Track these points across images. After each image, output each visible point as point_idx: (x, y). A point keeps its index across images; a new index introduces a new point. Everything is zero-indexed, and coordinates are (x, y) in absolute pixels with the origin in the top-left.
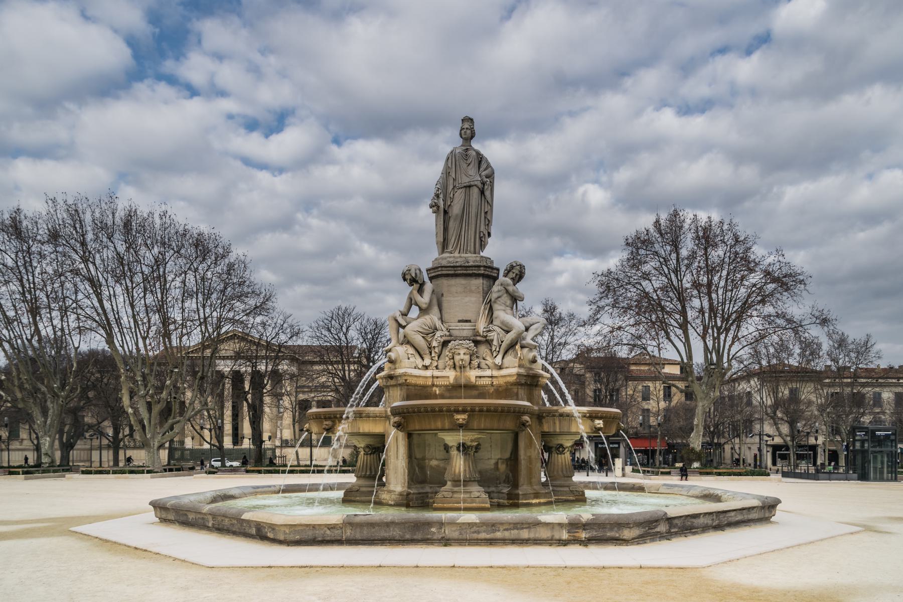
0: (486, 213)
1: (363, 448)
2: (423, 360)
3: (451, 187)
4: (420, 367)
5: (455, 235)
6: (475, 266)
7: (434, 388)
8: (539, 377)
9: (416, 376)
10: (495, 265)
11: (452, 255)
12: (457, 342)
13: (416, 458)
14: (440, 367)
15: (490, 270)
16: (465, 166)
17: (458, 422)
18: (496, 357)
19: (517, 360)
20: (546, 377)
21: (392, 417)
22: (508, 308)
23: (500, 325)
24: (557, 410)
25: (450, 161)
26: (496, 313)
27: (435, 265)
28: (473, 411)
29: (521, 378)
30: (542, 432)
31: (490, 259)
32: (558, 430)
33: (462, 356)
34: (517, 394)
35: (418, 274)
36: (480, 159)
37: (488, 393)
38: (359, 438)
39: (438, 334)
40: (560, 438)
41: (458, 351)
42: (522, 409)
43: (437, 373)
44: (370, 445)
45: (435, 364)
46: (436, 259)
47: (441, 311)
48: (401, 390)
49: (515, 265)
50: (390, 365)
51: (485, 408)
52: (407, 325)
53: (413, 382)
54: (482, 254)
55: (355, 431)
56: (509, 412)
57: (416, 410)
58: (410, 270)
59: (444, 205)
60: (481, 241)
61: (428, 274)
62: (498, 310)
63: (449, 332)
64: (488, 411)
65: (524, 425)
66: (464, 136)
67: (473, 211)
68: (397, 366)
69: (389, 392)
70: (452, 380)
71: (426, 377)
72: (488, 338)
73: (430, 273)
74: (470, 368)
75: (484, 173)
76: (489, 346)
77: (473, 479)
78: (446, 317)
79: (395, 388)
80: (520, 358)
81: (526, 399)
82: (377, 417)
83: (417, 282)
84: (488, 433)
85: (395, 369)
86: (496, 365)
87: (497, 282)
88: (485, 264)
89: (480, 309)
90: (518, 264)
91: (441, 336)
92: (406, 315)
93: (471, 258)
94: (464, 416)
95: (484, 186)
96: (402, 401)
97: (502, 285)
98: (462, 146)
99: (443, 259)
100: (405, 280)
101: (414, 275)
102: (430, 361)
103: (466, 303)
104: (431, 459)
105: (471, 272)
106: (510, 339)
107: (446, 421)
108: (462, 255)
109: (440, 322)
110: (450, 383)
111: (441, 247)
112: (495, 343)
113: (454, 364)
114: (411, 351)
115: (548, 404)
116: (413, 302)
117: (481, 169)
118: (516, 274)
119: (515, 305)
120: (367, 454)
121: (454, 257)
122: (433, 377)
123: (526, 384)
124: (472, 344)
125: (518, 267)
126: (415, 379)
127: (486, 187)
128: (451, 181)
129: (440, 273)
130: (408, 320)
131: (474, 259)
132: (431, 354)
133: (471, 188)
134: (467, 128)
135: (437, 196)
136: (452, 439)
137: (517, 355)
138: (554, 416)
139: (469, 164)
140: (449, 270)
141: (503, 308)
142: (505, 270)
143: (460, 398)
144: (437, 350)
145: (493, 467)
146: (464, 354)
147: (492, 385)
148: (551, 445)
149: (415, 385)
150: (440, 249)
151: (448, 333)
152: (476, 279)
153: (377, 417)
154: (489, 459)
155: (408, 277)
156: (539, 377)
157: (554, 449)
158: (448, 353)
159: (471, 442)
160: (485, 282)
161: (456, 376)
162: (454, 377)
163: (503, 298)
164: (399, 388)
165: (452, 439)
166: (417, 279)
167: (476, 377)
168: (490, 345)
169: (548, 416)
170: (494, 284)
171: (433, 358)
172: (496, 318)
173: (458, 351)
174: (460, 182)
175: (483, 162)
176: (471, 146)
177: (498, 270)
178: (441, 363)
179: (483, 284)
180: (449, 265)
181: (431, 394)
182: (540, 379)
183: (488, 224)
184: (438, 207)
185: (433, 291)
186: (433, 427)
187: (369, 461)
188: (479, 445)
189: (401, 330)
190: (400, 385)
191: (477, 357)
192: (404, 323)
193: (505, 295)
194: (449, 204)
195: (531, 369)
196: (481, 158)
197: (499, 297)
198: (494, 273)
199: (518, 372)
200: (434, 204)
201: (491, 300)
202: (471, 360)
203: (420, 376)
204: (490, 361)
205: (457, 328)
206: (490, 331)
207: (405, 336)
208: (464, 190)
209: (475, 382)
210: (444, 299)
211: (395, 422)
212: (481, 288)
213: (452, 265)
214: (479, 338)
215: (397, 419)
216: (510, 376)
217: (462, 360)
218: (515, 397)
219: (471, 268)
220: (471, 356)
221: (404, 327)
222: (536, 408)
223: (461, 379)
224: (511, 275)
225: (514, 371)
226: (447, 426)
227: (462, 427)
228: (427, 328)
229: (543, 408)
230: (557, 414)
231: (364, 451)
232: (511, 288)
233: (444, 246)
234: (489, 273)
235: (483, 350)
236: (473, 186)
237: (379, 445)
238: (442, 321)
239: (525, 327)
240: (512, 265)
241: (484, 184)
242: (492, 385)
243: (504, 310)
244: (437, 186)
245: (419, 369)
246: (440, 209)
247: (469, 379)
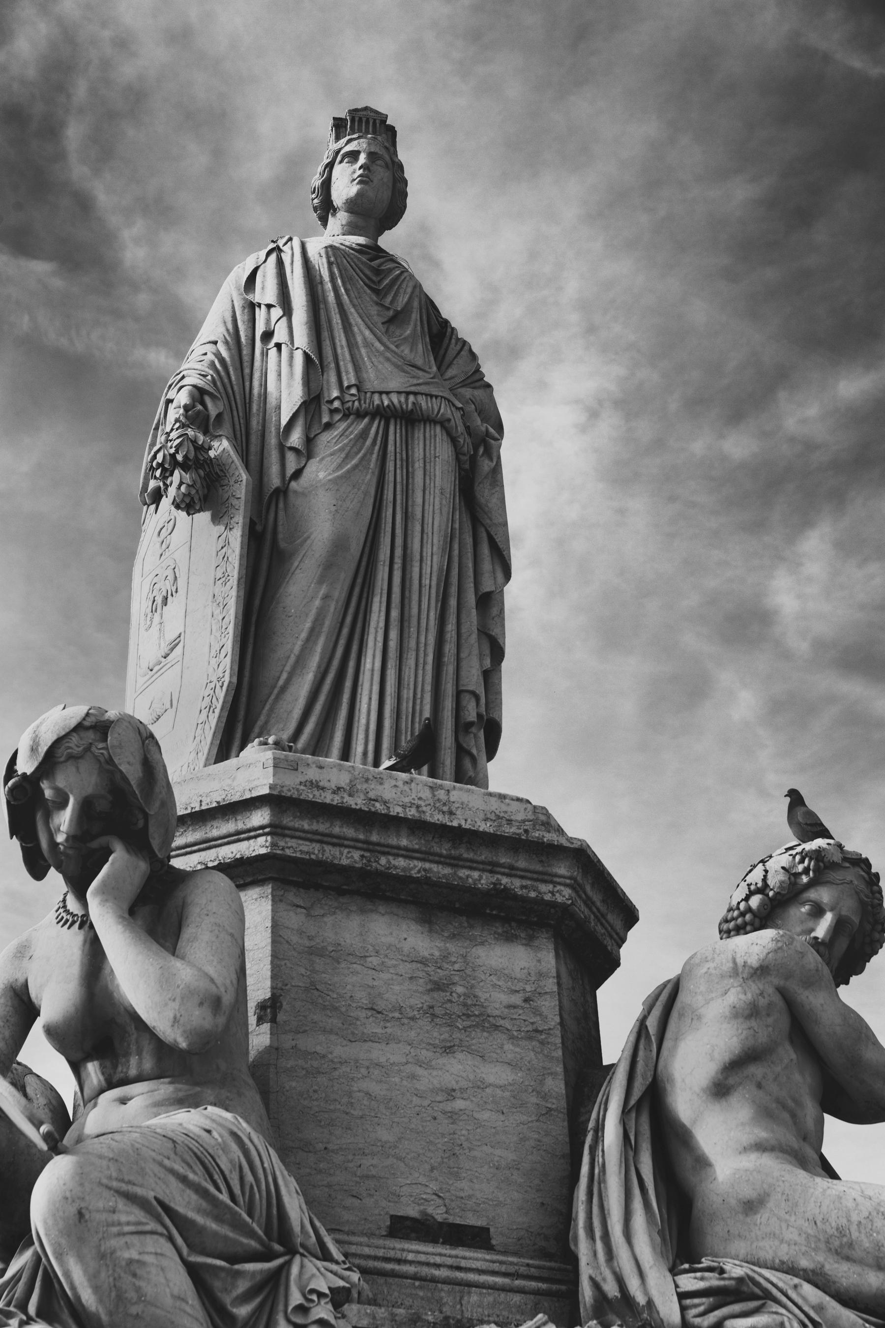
23: (804, 1263)
103: (451, 1094)
140: (323, 839)
193: (788, 1054)
219: (484, 855)
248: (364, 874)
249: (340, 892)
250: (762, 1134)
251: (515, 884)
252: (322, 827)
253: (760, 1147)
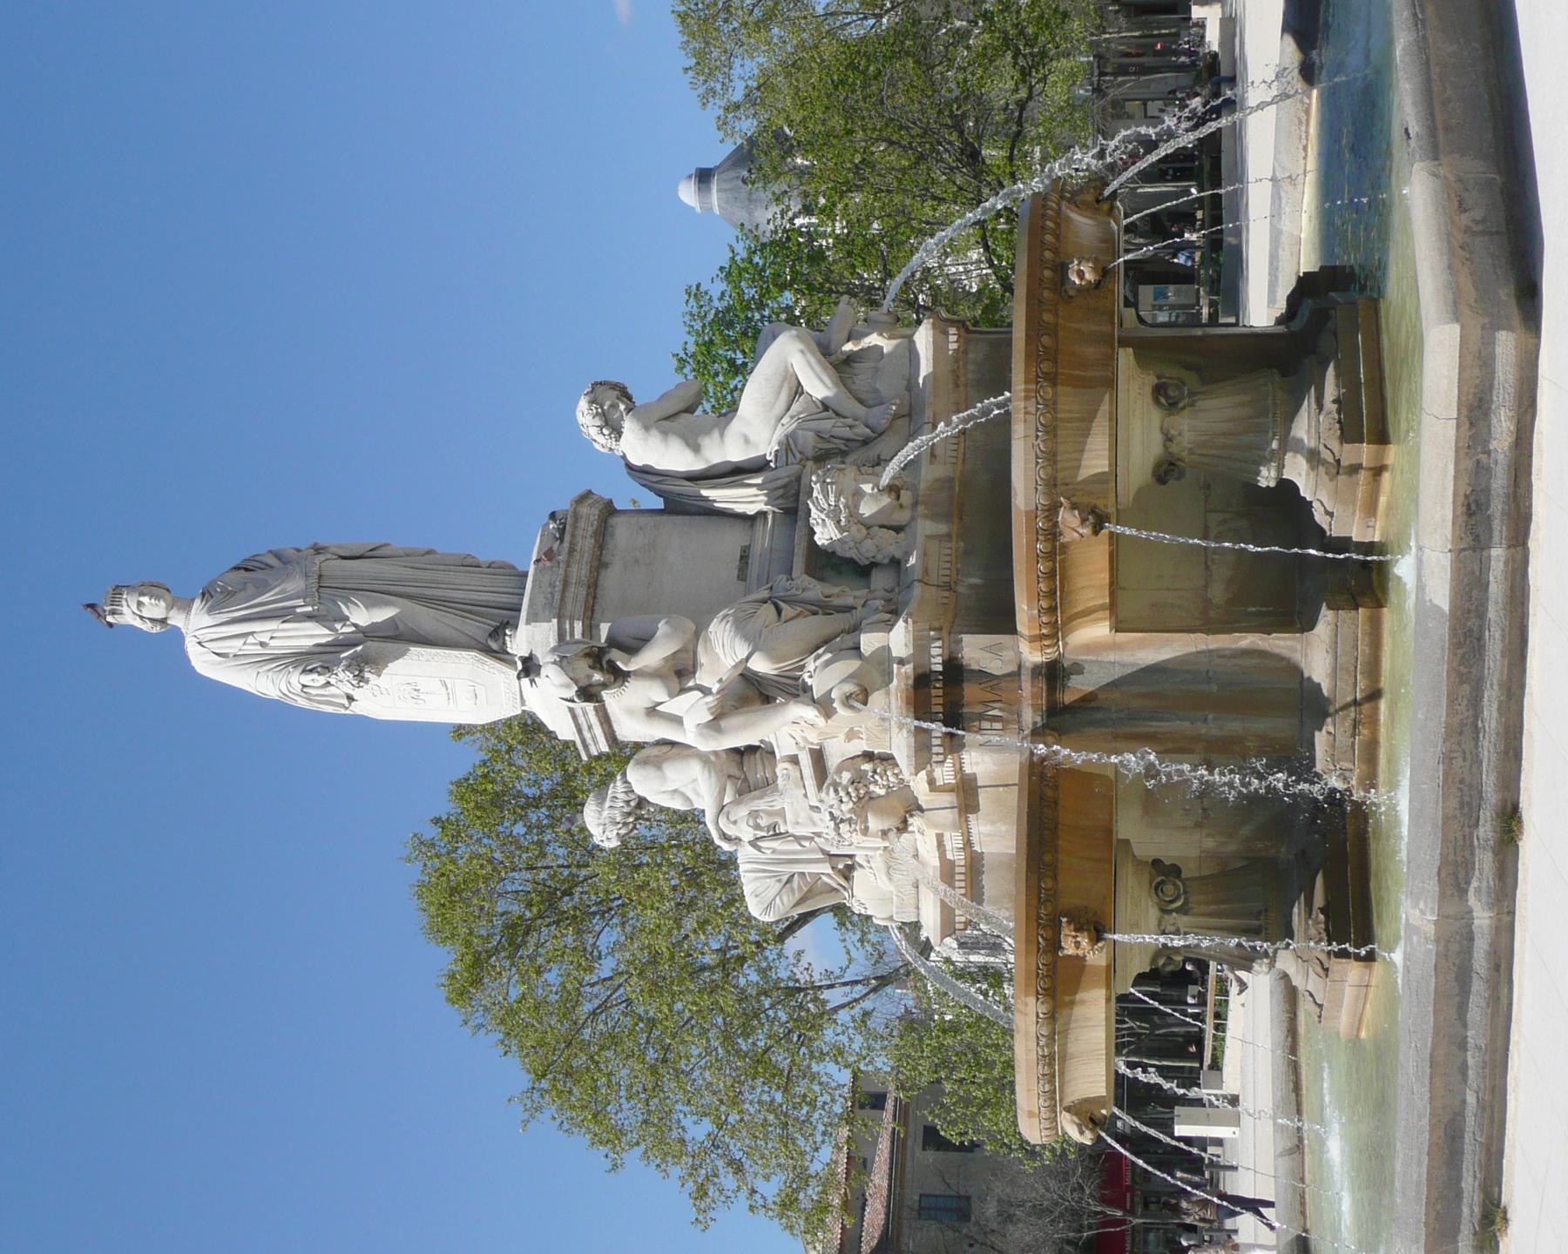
7: (961, 589)
104: (1207, 601)
161: (926, 517)
250: (716, 434)
253: (722, 435)
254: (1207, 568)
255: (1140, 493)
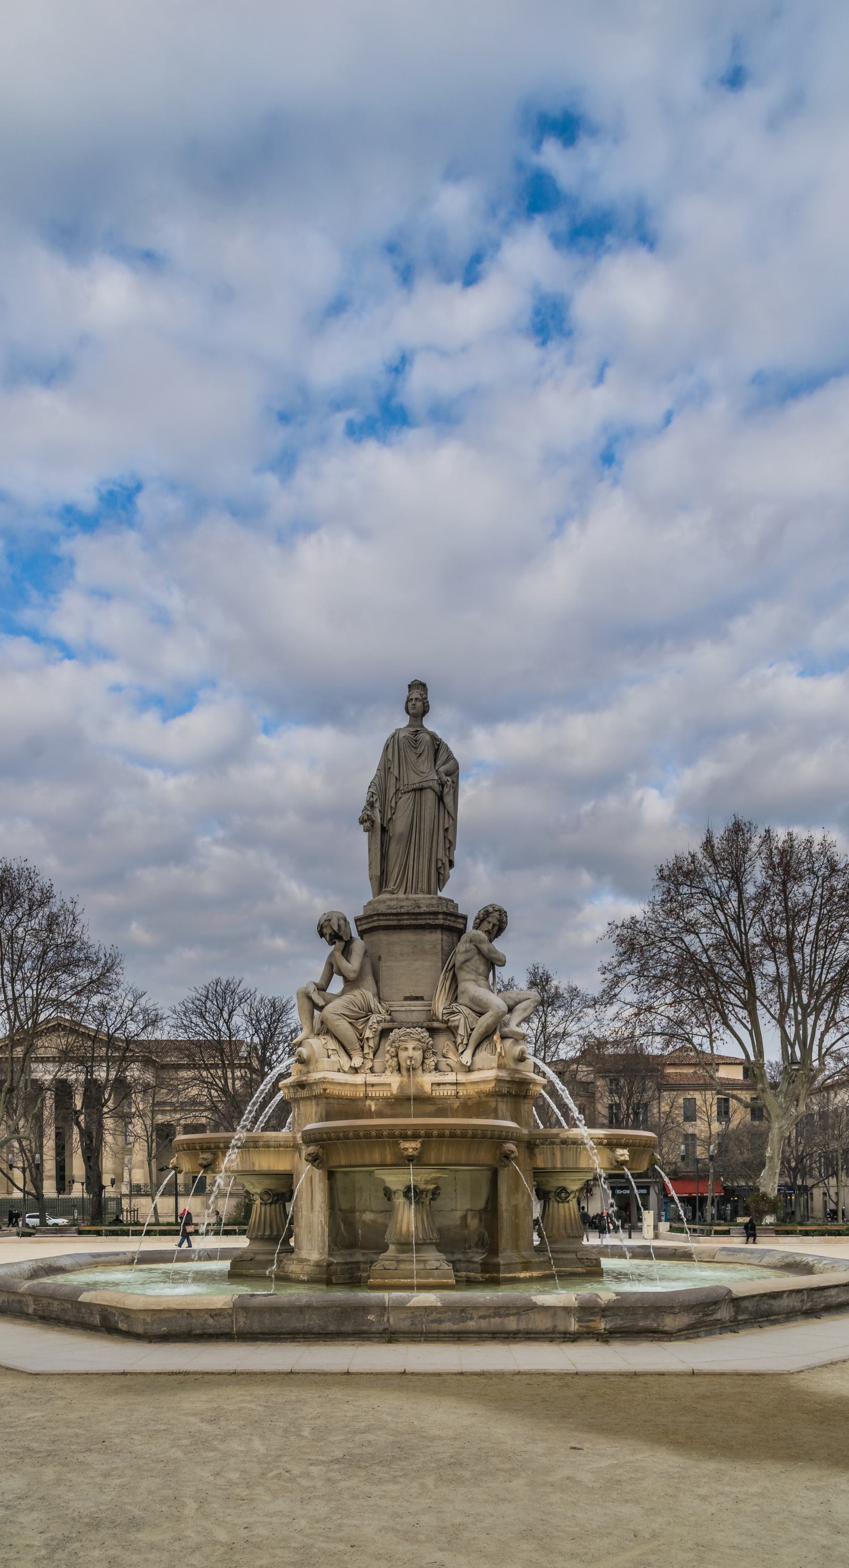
0: (446, 830)
1: (261, 1195)
2: (351, 1059)
3: (392, 791)
4: (346, 1069)
5: (398, 865)
6: (430, 913)
7: (368, 1102)
8: (530, 1083)
9: (340, 1084)
10: (461, 911)
11: (394, 896)
12: (402, 1031)
13: (340, 1210)
14: (376, 1069)
15: (453, 919)
16: (414, 757)
17: (406, 1153)
18: (462, 1053)
19: (496, 1057)
20: (540, 1084)
21: (303, 1147)
22: (481, 977)
23: (469, 1004)
24: (557, 1135)
25: (390, 750)
26: (463, 986)
27: (369, 912)
28: (428, 1135)
29: (502, 1084)
30: (534, 1168)
31: (452, 901)
32: (559, 1165)
33: (410, 1052)
34: (496, 1110)
35: (343, 927)
36: (437, 747)
37: (451, 1108)
38: (253, 1179)
39: (374, 1018)
40: (561, 1177)
41: (404, 1045)
42: (504, 1133)
43: (372, 1079)
44: (270, 1190)
45: (369, 1064)
46: (370, 903)
47: (377, 982)
48: (317, 1105)
49: (491, 910)
50: (300, 1066)
51: (447, 1132)
52: (326, 1005)
53: (336, 1092)
54: (440, 894)
55: (248, 1169)
56: (484, 1137)
57: (341, 1135)
58: (330, 920)
59: (382, 818)
60: (439, 873)
61: (357, 927)
62: (466, 980)
63: (390, 1015)
64: (453, 1135)
65: (507, 1157)
66: (411, 711)
67: (427, 826)
68: (311, 1068)
69: (299, 1109)
70: (395, 1089)
71: (356, 1085)
72: (450, 1024)
73: (361, 925)
74: (423, 1070)
75: (442, 769)
76: (451, 1036)
77: (428, 1241)
78: (385, 992)
79: (308, 1103)
80: (500, 1054)
81: (509, 1117)
82: (280, 1146)
83: (340, 938)
84: (451, 1170)
85: (309, 1072)
86: (462, 1065)
87: (464, 938)
88: (445, 909)
89: (438, 979)
90: (497, 908)
91: (378, 1022)
92: (324, 990)
93: (424, 901)
94: (416, 1144)
95: (443, 788)
96: (319, 1121)
97: (471, 941)
98: (409, 726)
99: (380, 902)
100: (322, 935)
101: (336, 928)
102: (362, 1060)
104: (364, 1211)
105: (423, 922)
106: (485, 1025)
107: (388, 1152)
108: (411, 896)
109: (376, 1000)
110: (392, 1094)
111: (377, 883)
112: (461, 1031)
113: (399, 1064)
114: (332, 1044)
115: (542, 1127)
116: (335, 969)
117: (438, 763)
118: (494, 925)
119: (491, 973)
120: (266, 1204)
121: (397, 899)
122: (366, 1085)
123: (509, 1094)
124: (426, 1034)
125: (496, 914)
126: (339, 1088)
127: (446, 790)
128: (393, 781)
129: (375, 924)
130: (328, 997)
131: (429, 902)
132: (363, 1050)
133: (424, 791)
134: (416, 699)
135: (371, 805)
136: (396, 1179)
137: (496, 1049)
138: (553, 1143)
139: (420, 754)
141: (473, 976)
142: (476, 919)
143: (409, 1116)
144: (371, 1043)
145: (458, 1222)
146: (414, 1049)
147: (457, 1096)
148: (548, 1188)
149: (339, 1098)
150: (376, 888)
151: (388, 1018)
152: (431, 932)
153: (280, 1146)
154: (452, 1210)
155: (327, 931)
156: (530, 1083)
157: (552, 1195)
158: (388, 1048)
159: (426, 1184)
160: (445, 937)
161: (402, 1082)
162: (398, 1084)
163: (473, 962)
164: (314, 1102)
165: (396, 1179)
166: (341, 934)
167: (432, 1084)
168: (453, 1034)
169: (543, 1144)
170: (459, 940)
171: (367, 1056)
172: (463, 993)
173: (404, 1045)
174: (406, 782)
175: (441, 752)
176: (422, 726)
177: (465, 918)
178: (378, 1064)
179: (442, 940)
180: (390, 911)
181: (363, 1110)
182: (531, 1086)
183: (449, 848)
184: (373, 822)
185: (366, 952)
186: (367, 1161)
187: (268, 1214)
188: (437, 1188)
189: (316, 1013)
190: (316, 1097)
191: (434, 1053)
192: (321, 1002)
193: (477, 957)
194: (389, 817)
195: (517, 1071)
196: (439, 745)
197: (467, 961)
198: (460, 923)
199: (498, 1076)
200: (366, 817)
201: (454, 966)
202: (424, 1058)
203: (346, 1084)
204: (453, 1059)
205: (403, 1009)
206: (453, 1013)
207: (322, 1023)
208: (412, 794)
209: (430, 1091)
210: (382, 964)
211: (309, 1155)
212: (439, 947)
213: (394, 911)
214: (436, 1024)
215: (312, 1149)
216: (484, 1082)
217: (411, 1058)
218: (493, 1115)
219: (423, 917)
220: (424, 1052)
221: (321, 1008)
222: (525, 1131)
223: (409, 1086)
224: (486, 926)
225: (492, 1074)
226: (389, 1159)
227: (412, 1160)
228: (356, 1009)
229: (536, 1132)
230: (557, 1141)
231: (261, 1199)
232: (485, 947)
233: (381, 882)
234: (452, 924)
235: (443, 1042)
236: (426, 788)
237: (284, 1190)
238: (379, 998)
239: (508, 1006)
240: (487, 911)
241: (442, 785)
242: (457, 1096)
243: (475, 981)
244: (371, 790)
245: (344, 1072)
246: (375, 826)
247: (422, 1087)
248: (398, 925)
249: (395, 929)
251: (430, 922)
252: (388, 918)
254: (382, 1212)
255: (383, 1181)
